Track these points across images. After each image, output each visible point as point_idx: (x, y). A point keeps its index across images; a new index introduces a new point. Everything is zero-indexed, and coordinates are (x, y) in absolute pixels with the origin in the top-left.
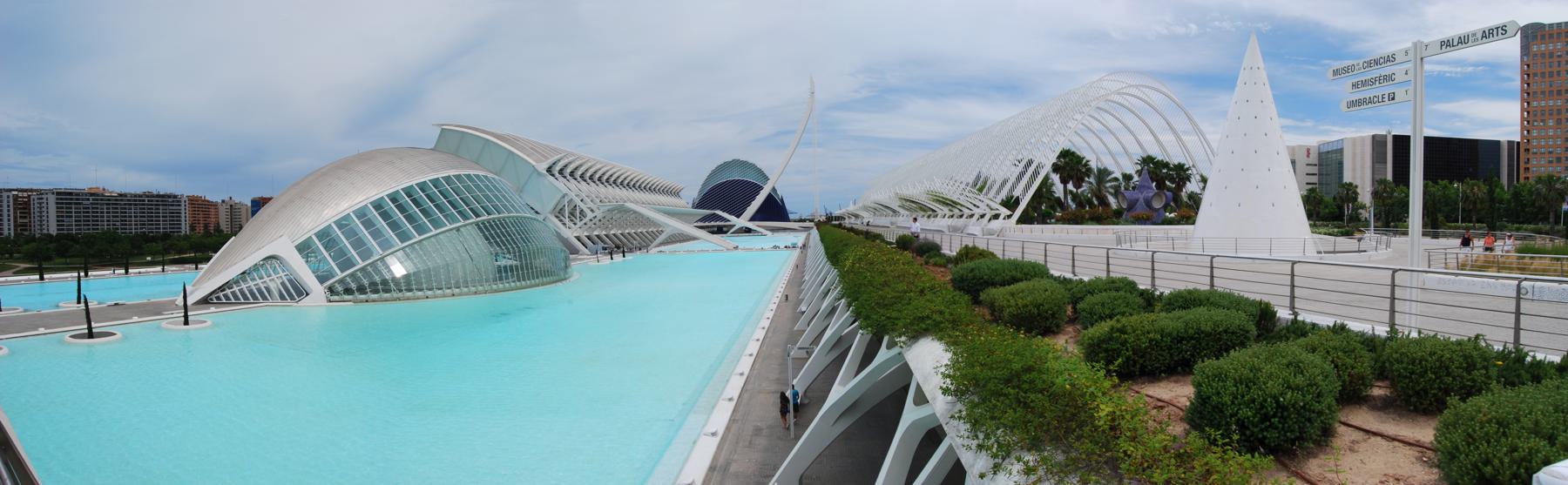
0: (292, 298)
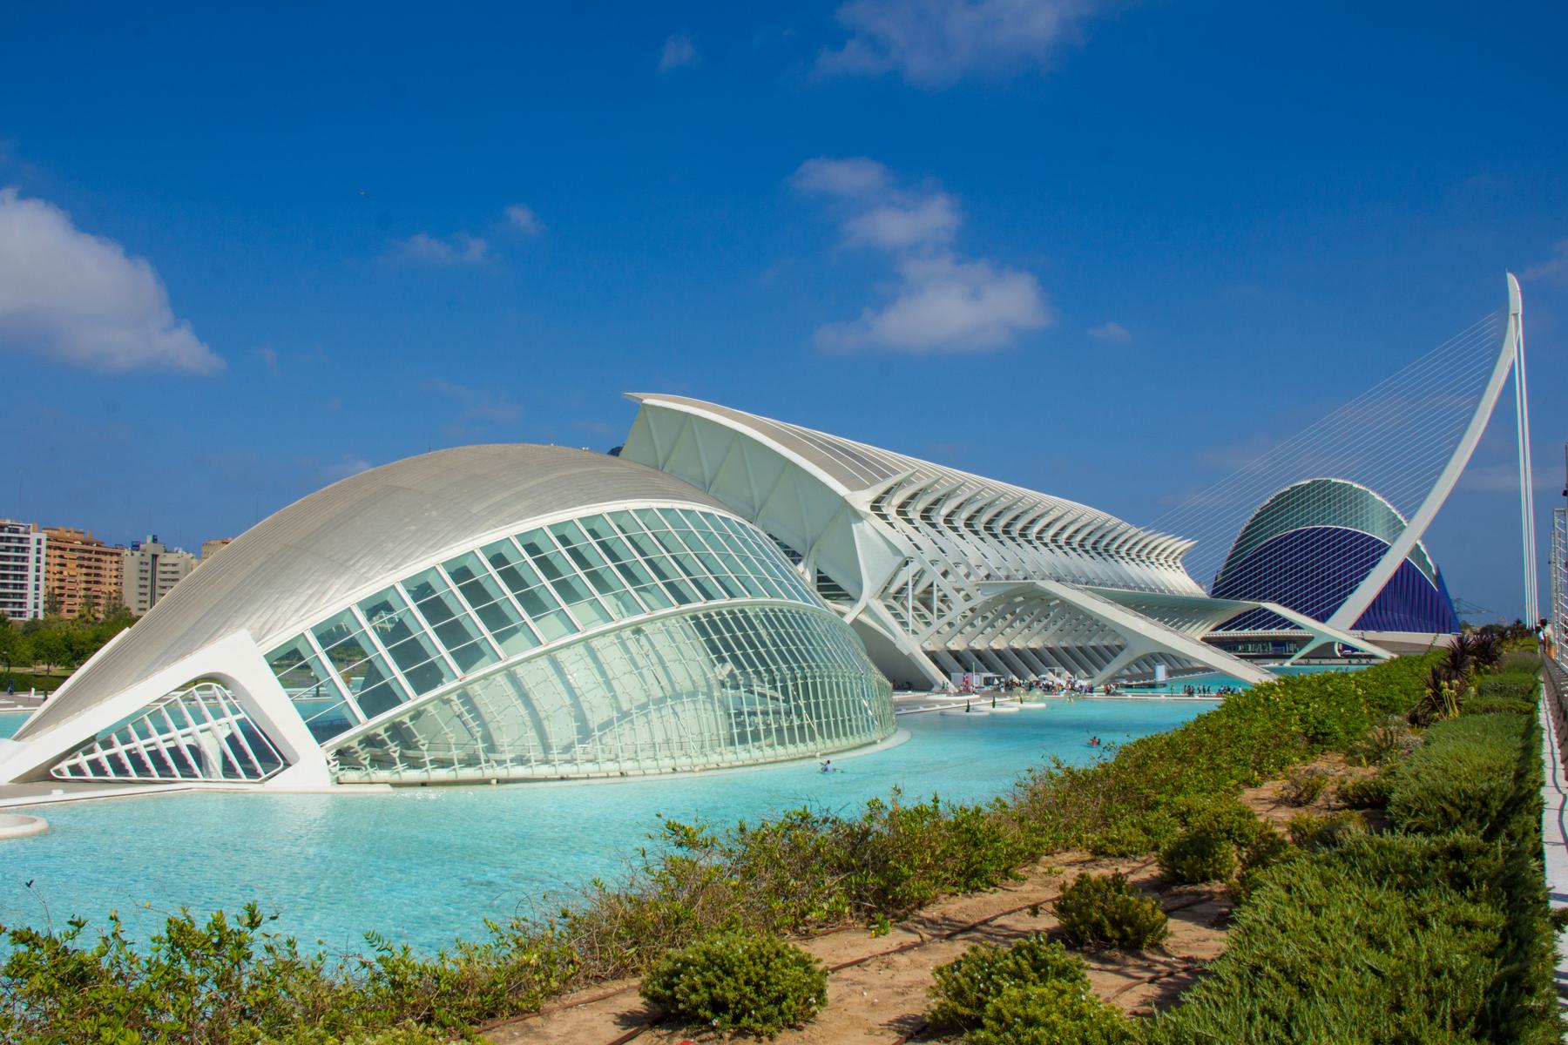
0: (252, 773)
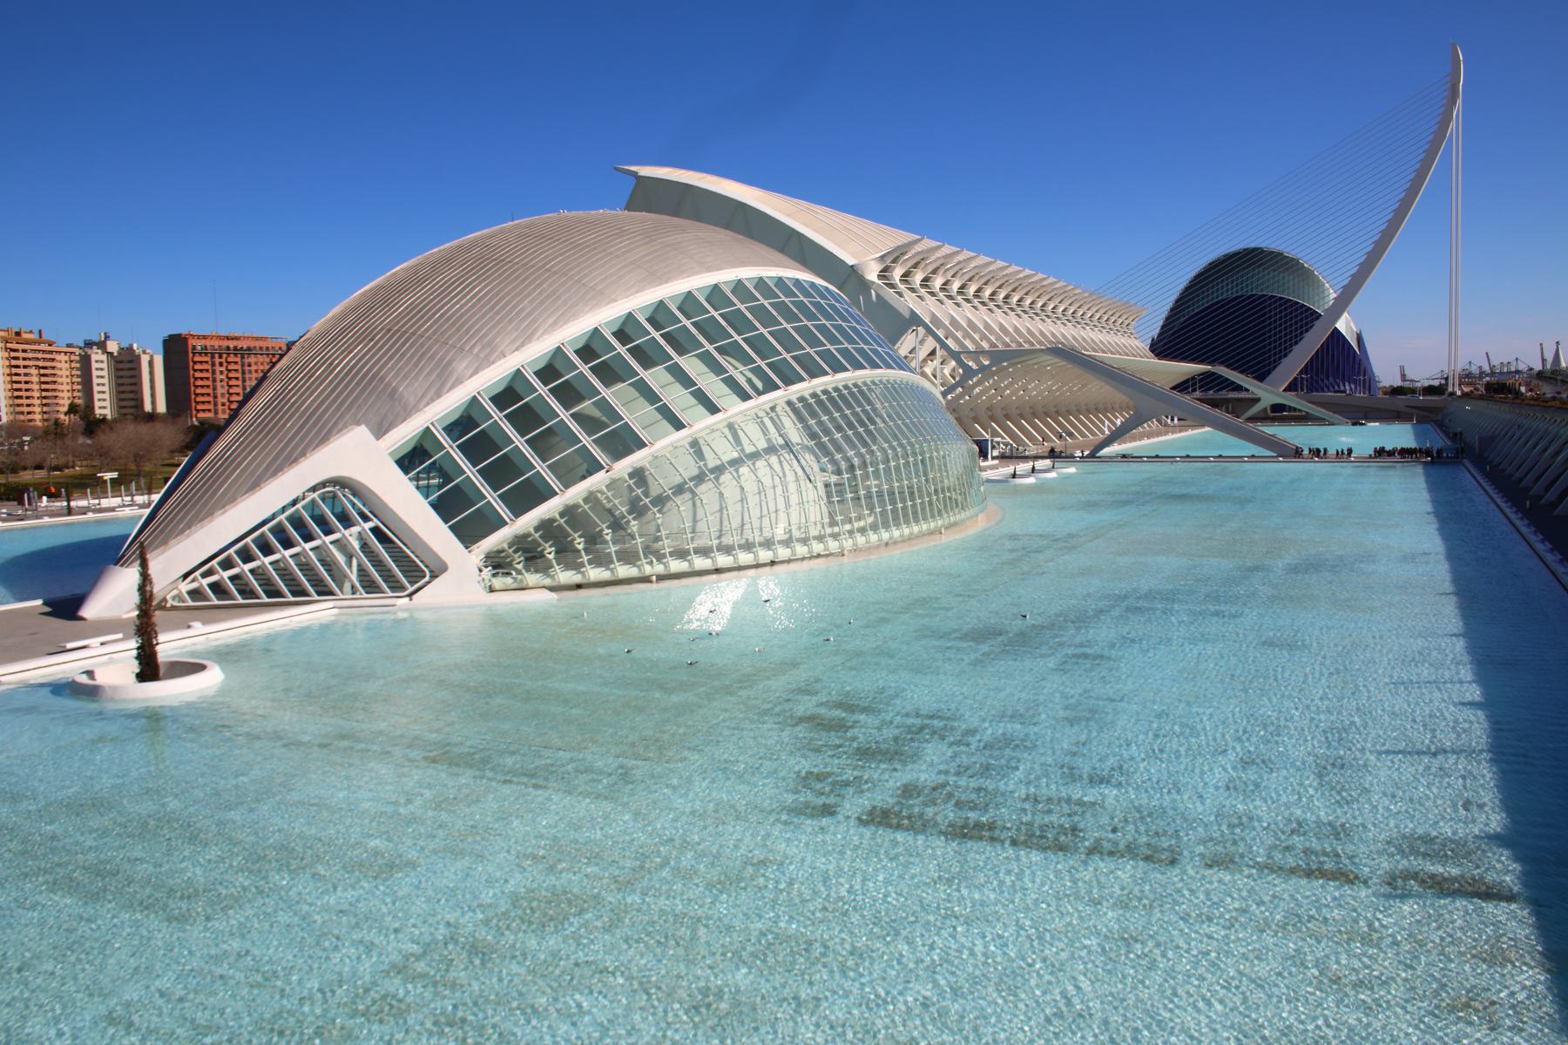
0: (396, 587)
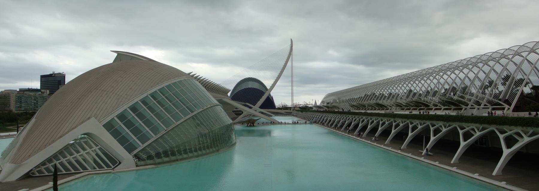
0: (108, 166)
